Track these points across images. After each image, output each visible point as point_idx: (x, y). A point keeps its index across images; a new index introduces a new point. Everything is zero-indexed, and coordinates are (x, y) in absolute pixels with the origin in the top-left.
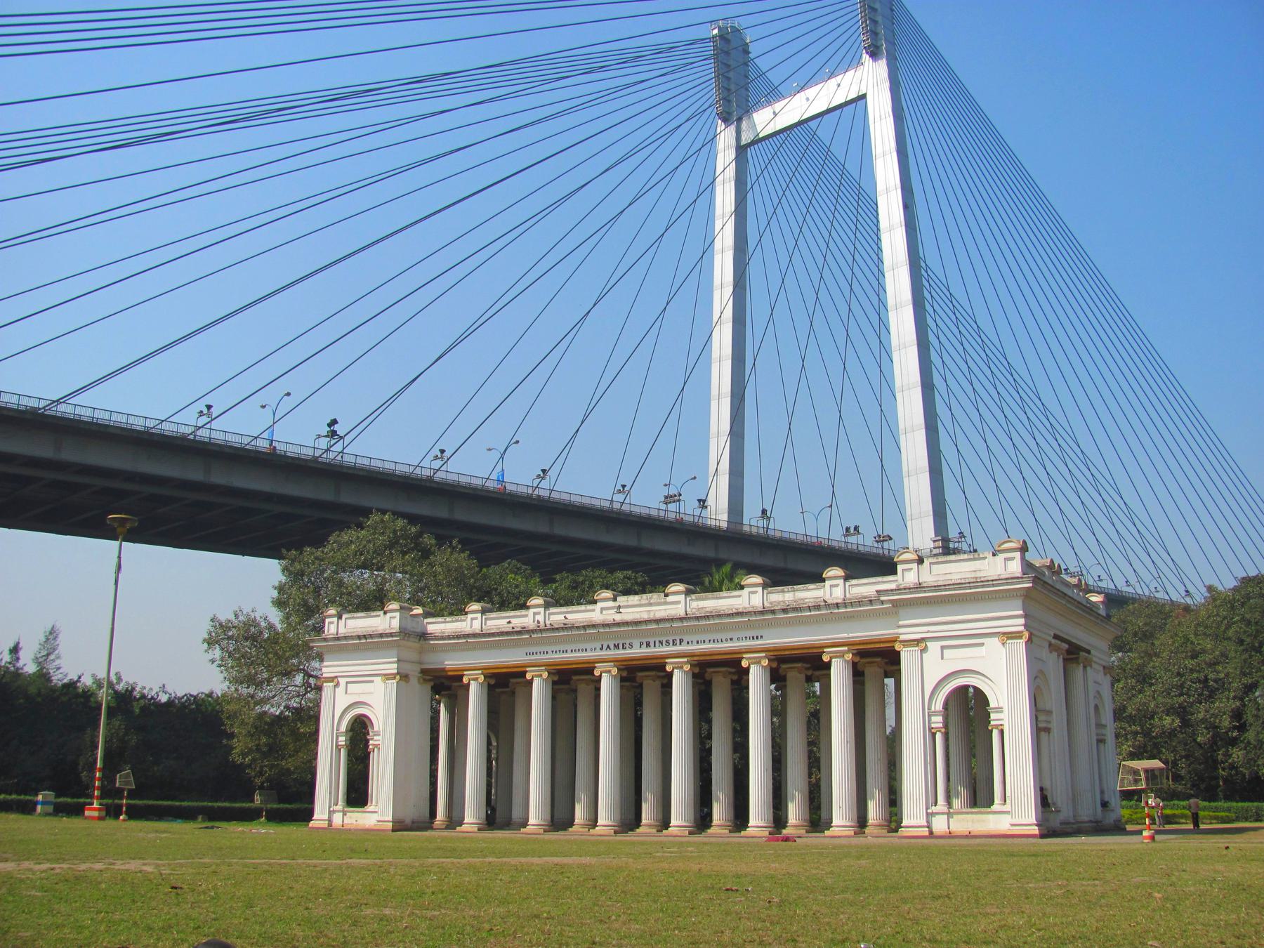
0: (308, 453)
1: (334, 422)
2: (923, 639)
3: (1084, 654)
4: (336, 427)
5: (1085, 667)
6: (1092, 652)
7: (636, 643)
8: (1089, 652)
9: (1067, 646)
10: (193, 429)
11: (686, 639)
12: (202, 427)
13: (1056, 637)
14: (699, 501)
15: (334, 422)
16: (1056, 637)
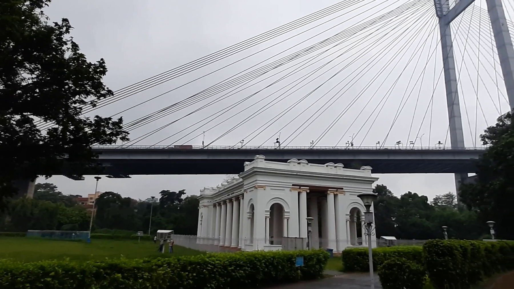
0: (273, 148)
1: (277, 139)
2: (247, 189)
3: (330, 189)
4: (278, 140)
5: (335, 196)
6: (344, 188)
7: (230, 193)
8: (342, 189)
9: (308, 188)
10: (241, 147)
11: (235, 192)
12: (244, 146)
13: (293, 185)
14: (410, 142)
15: (277, 139)
16: (293, 185)
